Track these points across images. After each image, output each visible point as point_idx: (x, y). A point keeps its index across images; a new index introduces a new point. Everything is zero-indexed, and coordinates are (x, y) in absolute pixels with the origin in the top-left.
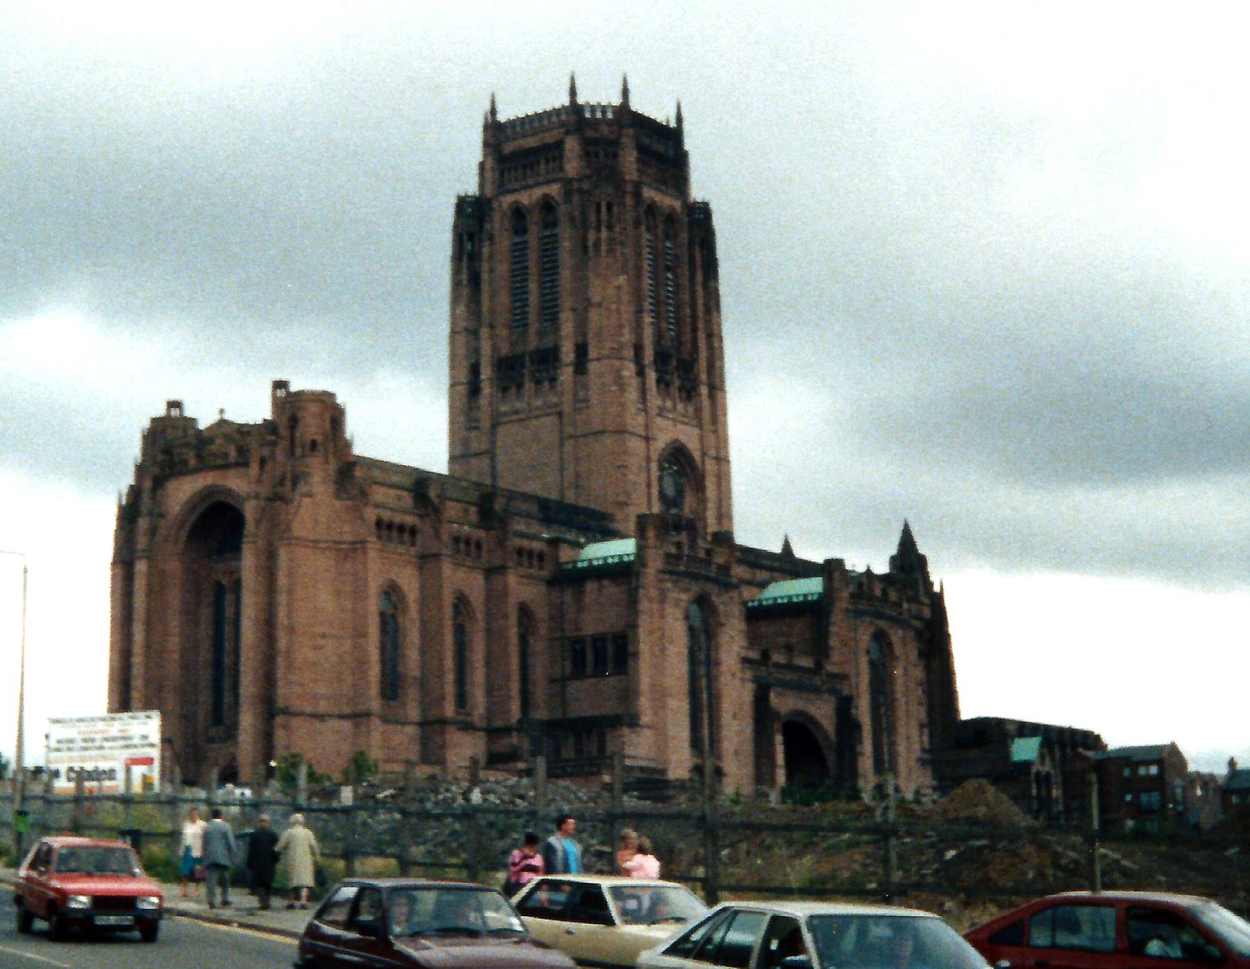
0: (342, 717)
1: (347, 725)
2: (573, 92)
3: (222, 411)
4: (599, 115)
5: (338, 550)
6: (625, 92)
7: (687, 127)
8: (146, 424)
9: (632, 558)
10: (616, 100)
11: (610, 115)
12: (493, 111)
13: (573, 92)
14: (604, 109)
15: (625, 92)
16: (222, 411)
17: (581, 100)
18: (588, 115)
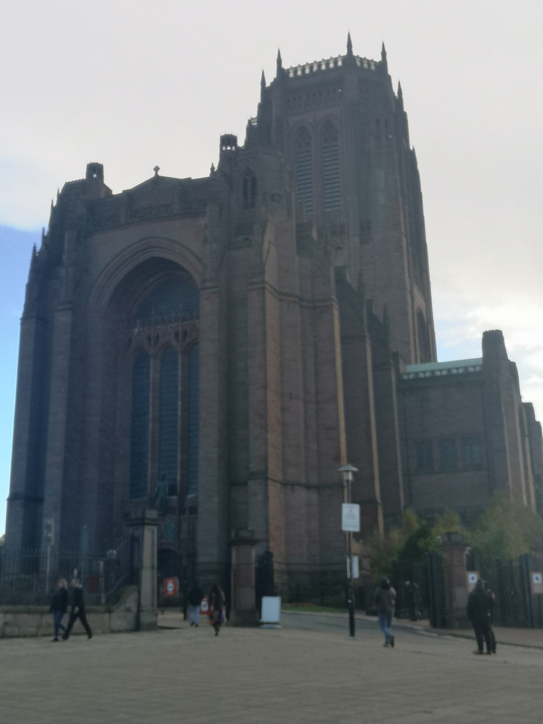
0: (308, 487)
1: (314, 496)
2: (349, 46)
3: (157, 169)
4: (366, 66)
5: (302, 307)
6: (384, 54)
7: (404, 96)
8: (61, 187)
9: (478, 369)
10: (378, 58)
11: (373, 68)
12: (279, 61)
13: (349, 46)
14: (369, 62)
15: (384, 54)
16: (157, 169)
17: (355, 54)
18: (358, 63)
